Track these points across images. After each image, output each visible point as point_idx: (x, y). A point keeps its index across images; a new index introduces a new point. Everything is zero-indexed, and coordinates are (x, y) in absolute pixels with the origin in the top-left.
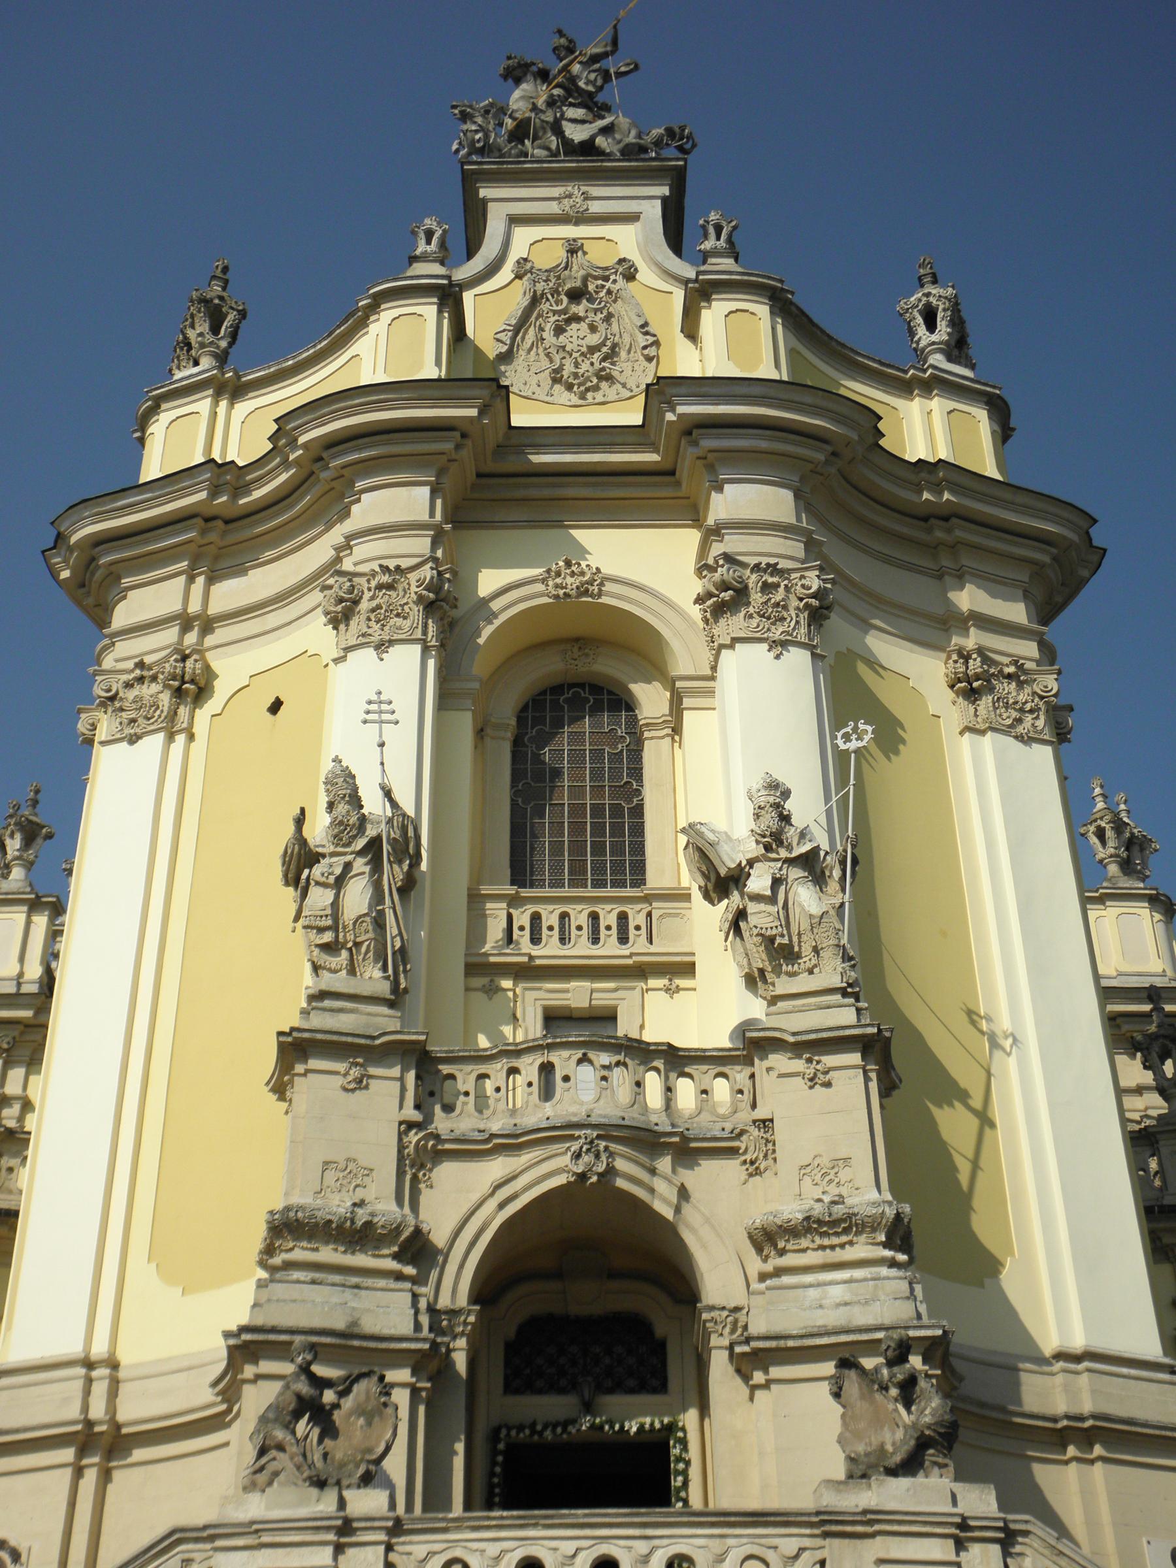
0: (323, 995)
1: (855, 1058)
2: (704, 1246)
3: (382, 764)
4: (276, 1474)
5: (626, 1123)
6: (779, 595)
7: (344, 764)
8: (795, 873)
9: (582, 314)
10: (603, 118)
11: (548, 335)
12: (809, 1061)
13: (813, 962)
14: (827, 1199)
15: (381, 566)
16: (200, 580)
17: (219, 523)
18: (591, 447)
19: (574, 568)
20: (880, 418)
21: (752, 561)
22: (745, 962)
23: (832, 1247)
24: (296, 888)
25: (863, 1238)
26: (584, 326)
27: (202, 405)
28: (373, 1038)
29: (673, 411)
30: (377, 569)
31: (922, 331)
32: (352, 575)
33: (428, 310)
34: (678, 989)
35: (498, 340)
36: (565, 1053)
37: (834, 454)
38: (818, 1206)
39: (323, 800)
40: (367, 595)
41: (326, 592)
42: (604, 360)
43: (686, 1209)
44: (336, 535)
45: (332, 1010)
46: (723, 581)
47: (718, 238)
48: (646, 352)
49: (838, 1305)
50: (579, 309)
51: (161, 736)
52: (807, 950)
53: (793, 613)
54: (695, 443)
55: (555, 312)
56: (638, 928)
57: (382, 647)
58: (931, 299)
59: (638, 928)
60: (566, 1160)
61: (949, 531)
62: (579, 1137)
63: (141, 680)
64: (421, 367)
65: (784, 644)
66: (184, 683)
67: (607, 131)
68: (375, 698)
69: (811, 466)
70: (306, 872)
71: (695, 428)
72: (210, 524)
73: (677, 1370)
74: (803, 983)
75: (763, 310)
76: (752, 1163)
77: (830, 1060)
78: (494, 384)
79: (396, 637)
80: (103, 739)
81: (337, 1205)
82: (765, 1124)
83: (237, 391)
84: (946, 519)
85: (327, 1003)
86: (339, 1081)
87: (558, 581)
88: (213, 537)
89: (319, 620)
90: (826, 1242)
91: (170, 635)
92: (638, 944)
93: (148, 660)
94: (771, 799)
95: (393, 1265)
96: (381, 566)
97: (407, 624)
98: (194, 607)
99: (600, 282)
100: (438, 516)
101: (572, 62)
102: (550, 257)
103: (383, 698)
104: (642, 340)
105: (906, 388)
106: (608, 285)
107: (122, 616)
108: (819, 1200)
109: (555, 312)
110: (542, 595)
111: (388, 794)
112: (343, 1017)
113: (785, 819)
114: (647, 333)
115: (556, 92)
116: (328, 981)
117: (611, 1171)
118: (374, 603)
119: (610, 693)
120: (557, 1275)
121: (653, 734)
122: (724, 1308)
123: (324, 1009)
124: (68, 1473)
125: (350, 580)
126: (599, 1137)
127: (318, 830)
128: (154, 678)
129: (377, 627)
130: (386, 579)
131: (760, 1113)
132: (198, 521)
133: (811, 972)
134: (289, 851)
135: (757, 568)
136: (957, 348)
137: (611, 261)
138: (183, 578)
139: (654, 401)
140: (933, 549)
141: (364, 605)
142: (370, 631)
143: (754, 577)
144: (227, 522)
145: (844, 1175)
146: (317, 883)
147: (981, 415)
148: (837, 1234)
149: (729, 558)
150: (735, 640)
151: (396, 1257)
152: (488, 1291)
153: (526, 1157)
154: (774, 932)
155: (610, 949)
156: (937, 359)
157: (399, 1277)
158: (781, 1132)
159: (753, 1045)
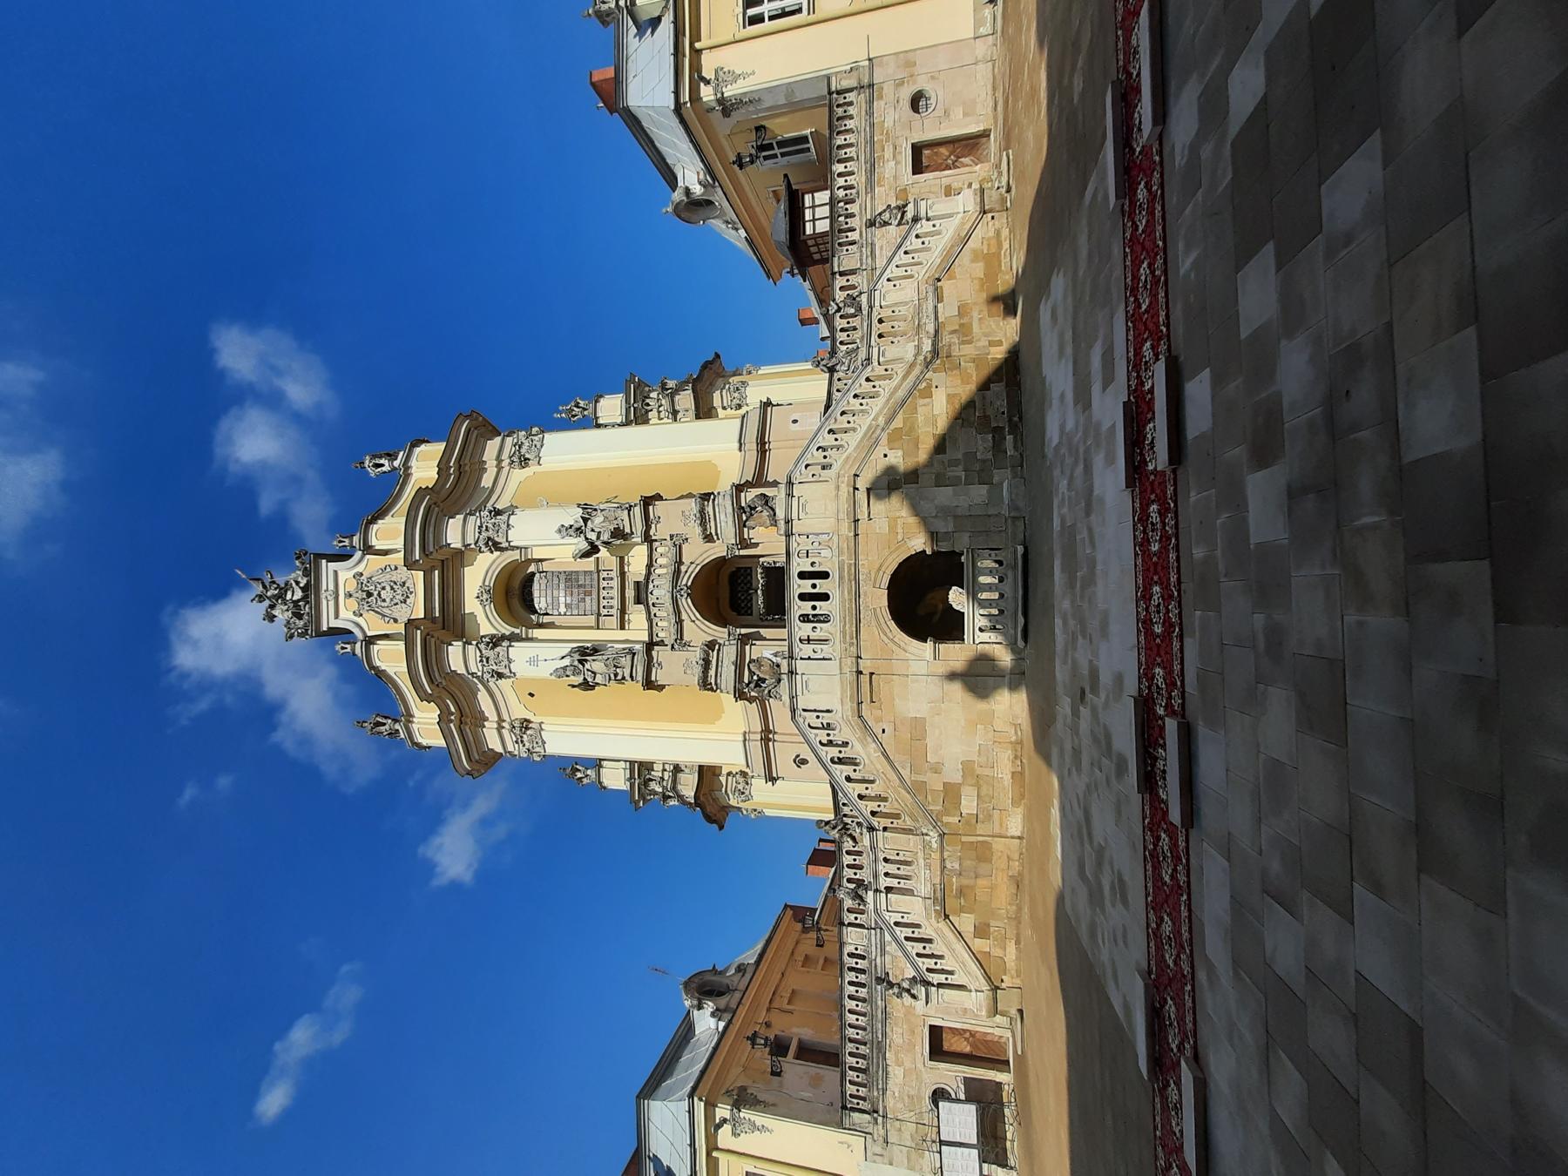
18: (432, 589)
27: (415, 727)
67: (297, 583)
75: (375, 527)
83: (410, 715)
91: (505, 732)
92: (613, 574)
105: (407, 476)
107: (499, 749)
116: (627, 675)
127: (580, 679)
136: (392, 456)
143: (484, 534)
147: (417, 450)
152: (721, 621)
155: (615, 583)
156: (396, 463)
159: (648, 539)
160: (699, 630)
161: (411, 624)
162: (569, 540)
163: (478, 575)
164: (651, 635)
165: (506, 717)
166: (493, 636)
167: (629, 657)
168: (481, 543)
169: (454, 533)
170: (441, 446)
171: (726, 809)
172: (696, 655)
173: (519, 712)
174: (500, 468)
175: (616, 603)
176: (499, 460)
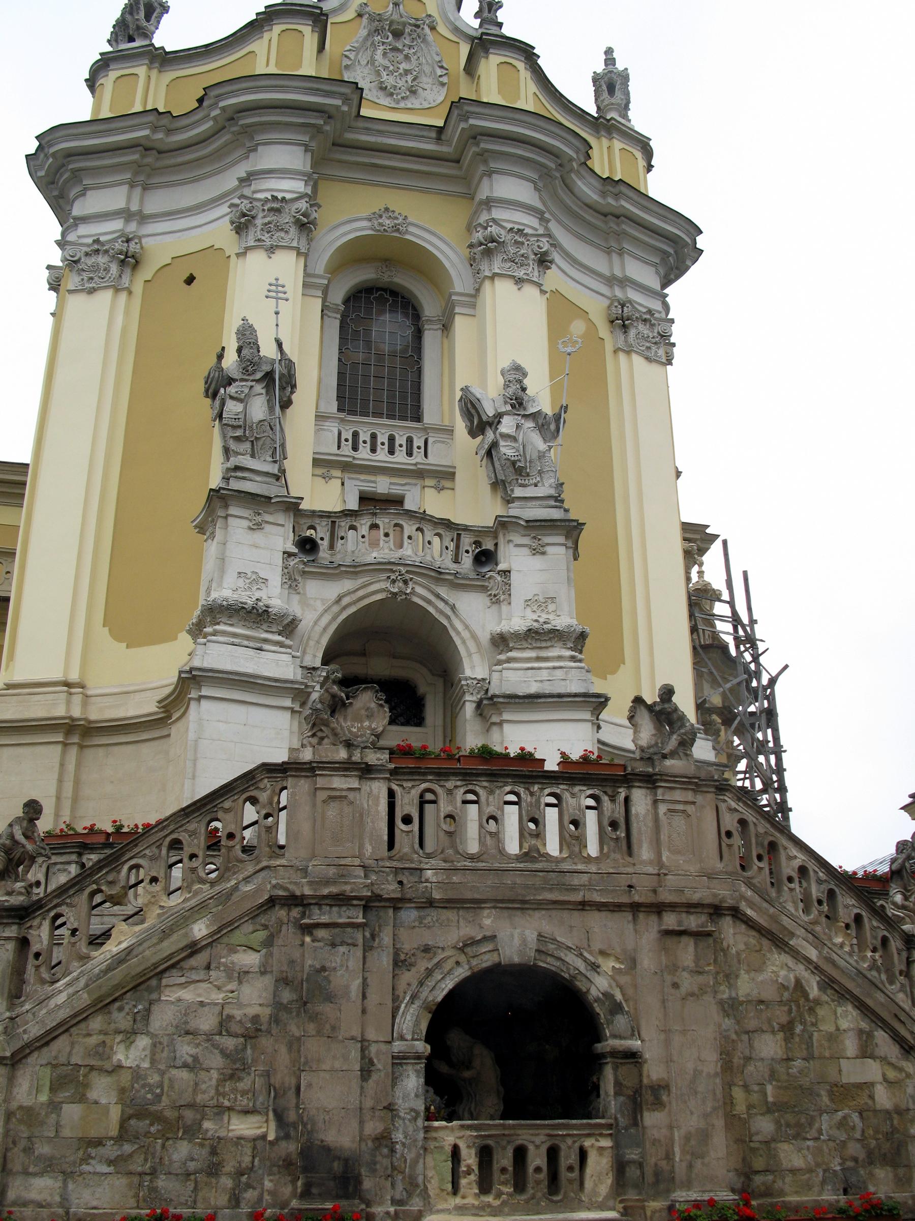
0: (237, 468)
2: (464, 642)
3: (277, 325)
4: (322, 739)
8: (530, 424)
11: (379, 56)
12: (534, 538)
13: (538, 479)
14: (542, 620)
15: (272, 196)
16: (138, 190)
17: (154, 152)
20: (591, 148)
21: (509, 226)
22: (493, 475)
23: (540, 648)
26: (401, 57)
27: (142, 71)
28: (271, 498)
29: (466, 120)
30: (270, 198)
31: (605, 95)
32: (252, 200)
33: (307, 30)
35: (346, 56)
36: (387, 520)
37: (560, 165)
38: (535, 624)
40: (261, 215)
41: (233, 209)
44: (241, 170)
45: (244, 478)
47: (489, 11)
48: (441, 79)
52: (534, 472)
54: (478, 145)
55: (383, 43)
56: (419, 448)
57: (271, 250)
58: (613, 75)
59: (419, 448)
60: (387, 585)
62: (396, 571)
63: (97, 251)
68: (274, 282)
70: (222, 391)
71: (477, 135)
72: (148, 152)
73: (433, 713)
74: (530, 492)
75: (521, 65)
76: (495, 596)
78: (355, 86)
79: (281, 244)
81: (247, 598)
82: (506, 573)
84: (618, 217)
85: (239, 474)
86: (245, 523)
87: (380, 221)
88: (148, 160)
89: (225, 226)
91: (117, 225)
93: (102, 239)
95: (279, 638)
96: (272, 196)
97: (287, 237)
98: (134, 208)
100: (308, 168)
103: (280, 282)
104: (439, 72)
106: (419, 30)
108: (536, 621)
109: (383, 43)
111: (280, 345)
112: (248, 483)
113: (524, 389)
114: (442, 67)
117: (413, 592)
118: (268, 219)
119: (403, 297)
120: (363, 654)
122: (475, 678)
123: (236, 477)
124: (59, 748)
125: (251, 203)
126: (407, 572)
129: (267, 236)
130: (275, 205)
132: (140, 148)
133: (536, 486)
135: (511, 229)
138: (125, 188)
139: (456, 112)
141: (259, 222)
142: (263, 238)
143: (509, 236)
144: (160, 152)
145: (551, 607)
146: (232, 398)
149: (494, 220)
150: (495, 275)
153: (360, 581)
154: (516, 458)
157: (281, 645)
164: (313, 514)
165: (150, 228)
167: (274, 469)
168: (493, 230)
172: (274, 596)
174: (611, 281)
176: (625, 282)
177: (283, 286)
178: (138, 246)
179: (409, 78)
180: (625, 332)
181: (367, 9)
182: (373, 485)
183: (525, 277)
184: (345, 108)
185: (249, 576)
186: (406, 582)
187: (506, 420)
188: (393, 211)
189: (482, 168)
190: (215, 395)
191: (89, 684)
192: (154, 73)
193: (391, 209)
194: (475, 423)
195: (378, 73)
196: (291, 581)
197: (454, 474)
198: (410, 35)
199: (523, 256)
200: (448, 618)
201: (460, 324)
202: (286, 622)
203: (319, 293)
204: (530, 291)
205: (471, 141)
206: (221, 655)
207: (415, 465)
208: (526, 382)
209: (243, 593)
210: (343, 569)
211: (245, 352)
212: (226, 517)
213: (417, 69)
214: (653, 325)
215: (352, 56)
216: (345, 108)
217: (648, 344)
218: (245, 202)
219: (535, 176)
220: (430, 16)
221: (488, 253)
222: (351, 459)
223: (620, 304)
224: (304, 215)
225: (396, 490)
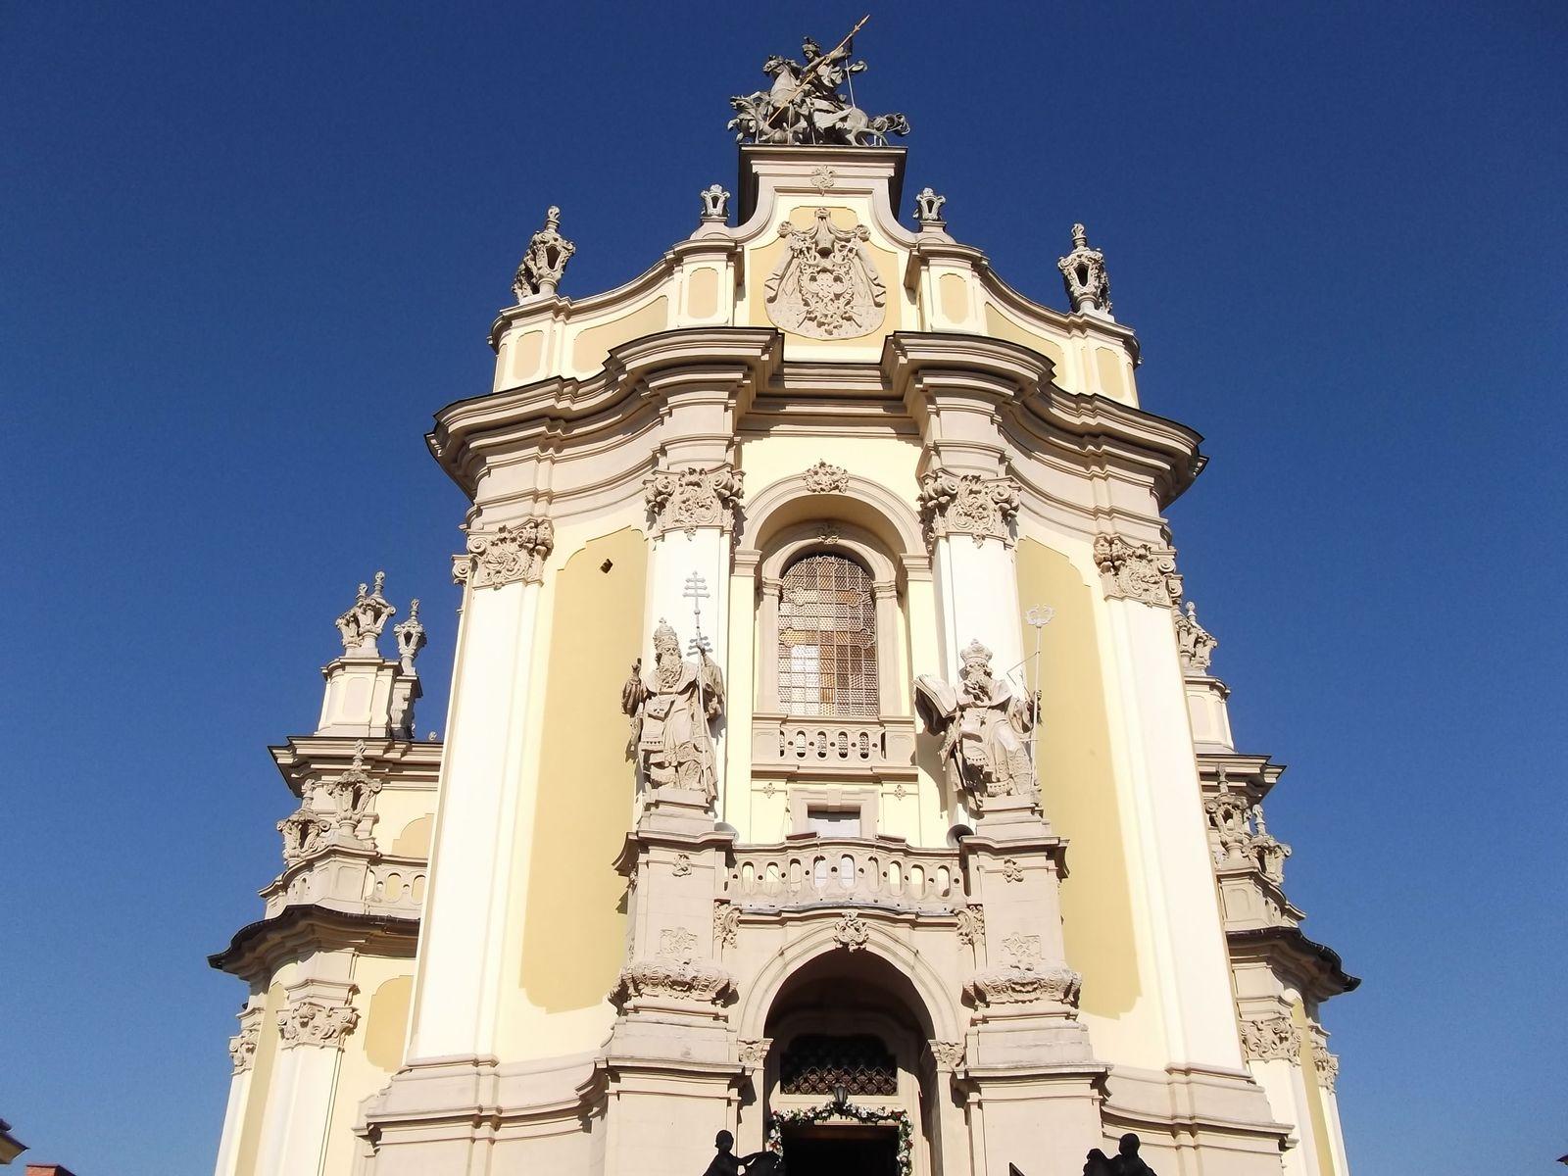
1: (1040, 859)
5: (879, 905)
6: (981, 499)
7: (669, 624)
8: (998, 714)
9: (830, 268)
10: (842, 109)
19: (828, 469)
21: (962, 473)
24: (632, 711)
25: (1046, 996)
28: (695, 837)
30: (687, 471)
32: (666, 474)
34: (905, 794)
39: (653, 653)
42: (848, 303)
43: (919, 969)
46: (943, 489)
47: (930, 212)
49: (1029, 1047)
50: (826, 263)
51: (520, 585)
53: (991, 513)
54: (921, 382)
56: (875, 745)
57: (690, 531)
58: (1083, 259)
61: (1098, 447)
63: (503, 540)
64: (713, 310)
65: (984, 538)
66: (537, 545)
69: (1003, 399)
70: (641, 704)
72: (557, 423)
76: (967, 935)
77: (1023, 861)
80: (475, 584)
86: (671, 869)
87: (816, 478)
90: (1020, 996)
91: (525, 507)
93: (510, 525)
94: (979, 660)
98: (542, 487)
99: (843, 243)
100: (729, 431)
101: (820, 63)
102: (806, 222)
104: (877, 290)
106: (849, 245)
110: (800, 489)
113: (989, 674)
114: (878, 285)
115: (807, 87)
116: (662, 793)
121: (883, 594)
125: (666, 478)
126: (859, 915)
127: (649, 677)
128: (514, 540)
130: (694, 478)
131: (972, 900)
133: (1009, 794)
134: (628, 691)
135: (965, 477)
137: (851, 227)
140: (1084, 460)
141: (676, 498)
142: (682, 518)
143: (965, 483)
144: (568, 421)
145: (1034, 948)
146: (650, 716)
148: (1028, 992)
151: (713, 1002)
155: (854, 764)
157: (716, 1017)
158: (988, 913)
160: (763, 966)
161: (776, 337)
162: (954, 666)
163: (878, 466)
166: (738, 494)
168: (944, 482)
169: (965, 426)
170: (1131, 400)
171: (261, 977)
173: (569, 537)
174: (1096, 513)
175: (811, 764)
177: (703, 581)
178: (548, 531)
179: (842, 306)
180: (1117, 574)
181: (790, 229)
182: (825, 796)
183: (985, 532)
184: (766, 357)
185: (675, 934)
186: (857, 930)
187: (968, 713)
188: (831, 466)
189: (931, 407)
190: (632, 711)
191: (502, 1060)
192: (559, 326)
193: (828, 464)
194: (935, 718)
195: (806, 304)
196: (726, 935)
197: (917, 775)
198: (841, 251)
199: (981, 506)
200: (913, 968)
201: (919, 591)
202: (719, 988)
203: (751, 572)
204: (993, 546)
205: (911, 378)
206: (645, 1039)
207: (871, 769)
208: (991, 665)
209: (668, 956)
210: (784, 915)
211: (665, 659)
212: (647, 863)
213: (850, 291)
214: (1150, 561)
215: (774, 284)
216: (766, 357)
217: (1145, 586)
218: (661, 477)
219: (992, 407)
220: (861, 226)
221: (942, 508)
222: (795, 769)
223: (1106, 540)
224: (725, 487)
225: (849, 801)
